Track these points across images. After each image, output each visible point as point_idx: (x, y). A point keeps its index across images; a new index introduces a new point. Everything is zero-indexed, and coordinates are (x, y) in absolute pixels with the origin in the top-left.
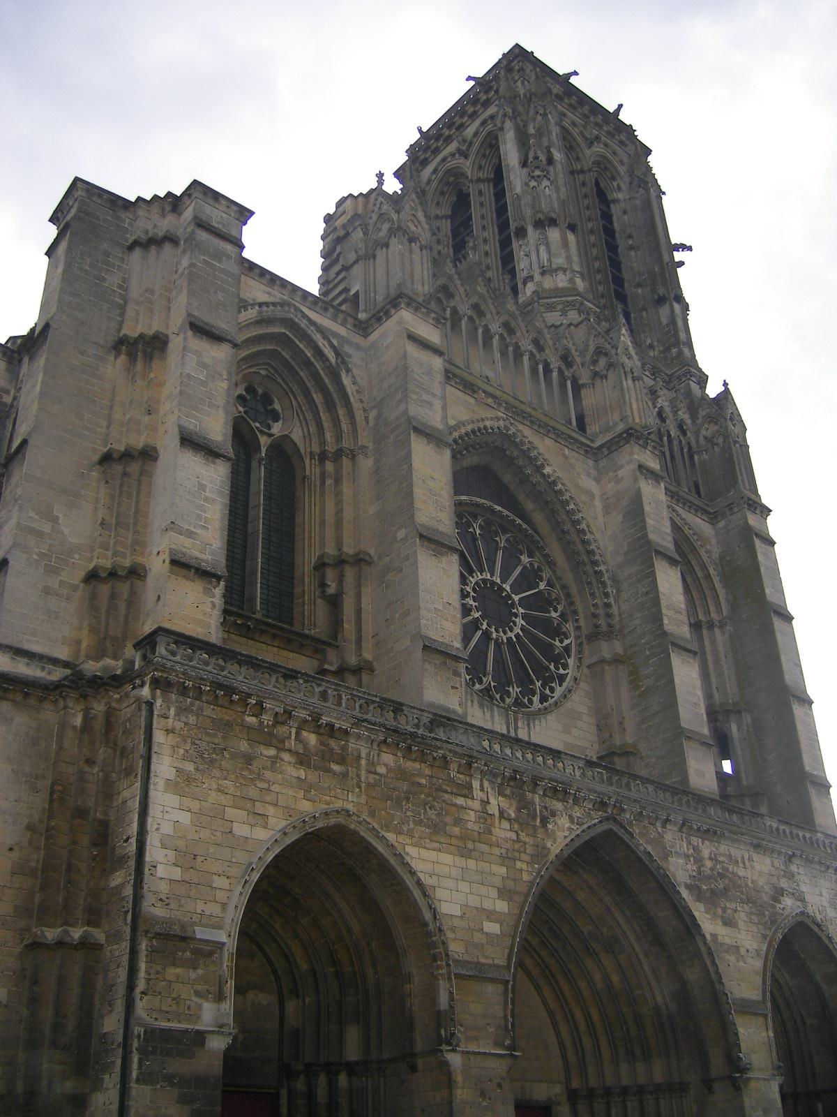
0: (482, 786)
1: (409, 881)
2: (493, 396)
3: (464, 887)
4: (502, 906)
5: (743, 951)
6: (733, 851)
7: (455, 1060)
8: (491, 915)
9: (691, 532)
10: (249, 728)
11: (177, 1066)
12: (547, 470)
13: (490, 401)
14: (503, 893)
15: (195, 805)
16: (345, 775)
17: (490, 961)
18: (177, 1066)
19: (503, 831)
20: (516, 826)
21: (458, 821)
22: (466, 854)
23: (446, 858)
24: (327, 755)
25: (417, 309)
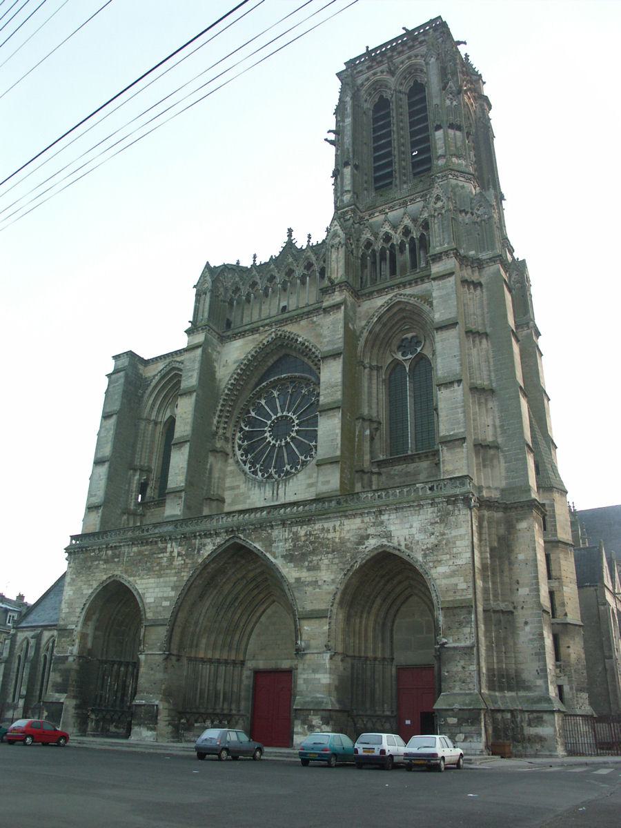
0: (171, 545)
1: (135, 593)
2: (267, 325)
3: (157, 590)
4: (173, 594)
5: (320, 583)
6: (326, 525)
7: (142, 657)
8: (166, 599)
9: (416, 299)
10: (93, 556)
11: (61, 666)
12: (300, 339)
13: (267, 328)
14: (174, 588)
15: (74, 588)
16: (119, 561)
17: (162, 618)
18: (61, 666)
19: (178, 562)
20: (185, 557)
21: (159, 564)
22: (159, 576)
23: (152, 580)
24: (114, 556)
25: (193, 332)
